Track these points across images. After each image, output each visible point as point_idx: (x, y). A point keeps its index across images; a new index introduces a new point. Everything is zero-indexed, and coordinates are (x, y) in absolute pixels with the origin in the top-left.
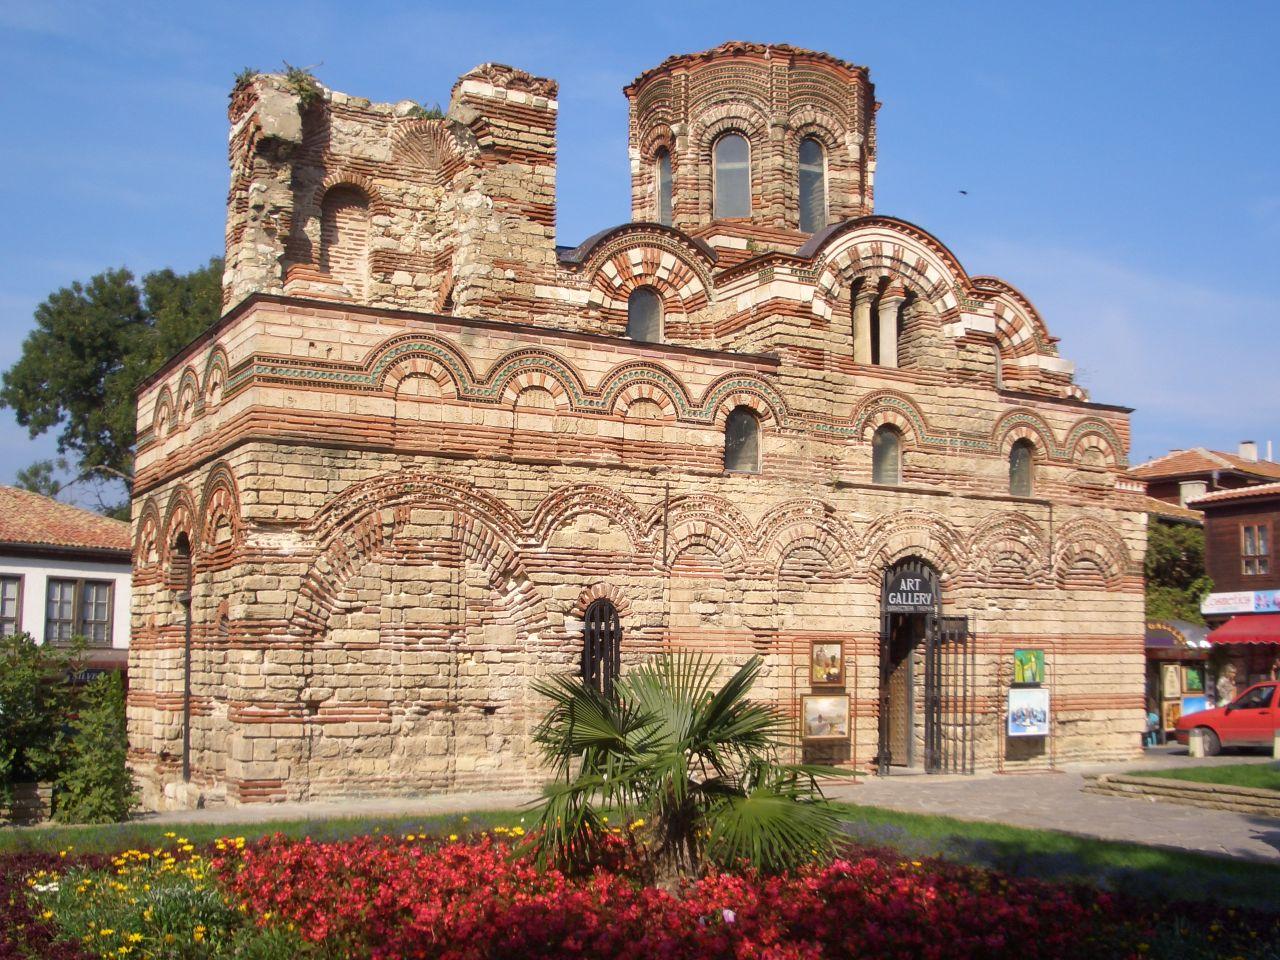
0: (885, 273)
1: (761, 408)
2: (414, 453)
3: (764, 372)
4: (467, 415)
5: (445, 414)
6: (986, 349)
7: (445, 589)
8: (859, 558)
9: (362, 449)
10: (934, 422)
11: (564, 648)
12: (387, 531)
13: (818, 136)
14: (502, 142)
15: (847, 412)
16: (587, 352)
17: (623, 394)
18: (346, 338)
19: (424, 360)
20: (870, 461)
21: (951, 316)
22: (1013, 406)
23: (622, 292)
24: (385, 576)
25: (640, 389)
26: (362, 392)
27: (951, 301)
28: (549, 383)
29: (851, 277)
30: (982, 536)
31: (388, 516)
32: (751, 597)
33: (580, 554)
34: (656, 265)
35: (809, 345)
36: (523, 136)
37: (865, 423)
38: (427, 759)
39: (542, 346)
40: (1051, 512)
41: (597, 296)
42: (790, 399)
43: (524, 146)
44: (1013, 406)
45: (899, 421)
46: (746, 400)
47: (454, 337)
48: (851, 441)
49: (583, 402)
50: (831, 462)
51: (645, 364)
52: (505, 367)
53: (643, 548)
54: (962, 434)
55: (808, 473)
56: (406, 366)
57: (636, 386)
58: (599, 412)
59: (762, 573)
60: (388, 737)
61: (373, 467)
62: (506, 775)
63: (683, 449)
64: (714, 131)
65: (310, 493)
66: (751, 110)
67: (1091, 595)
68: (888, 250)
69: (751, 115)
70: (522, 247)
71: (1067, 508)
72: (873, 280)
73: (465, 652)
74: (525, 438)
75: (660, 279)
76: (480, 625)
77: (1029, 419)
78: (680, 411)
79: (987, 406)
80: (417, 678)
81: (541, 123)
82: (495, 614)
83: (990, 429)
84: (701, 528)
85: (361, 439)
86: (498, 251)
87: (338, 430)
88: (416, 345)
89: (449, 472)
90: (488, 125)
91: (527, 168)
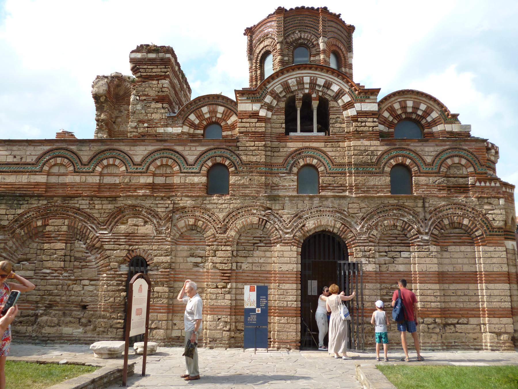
0: (307, 91)
1: (227, 163)
2: (52, 197)
3: (230, 146)
4: (77, 179)
5: (68, 179)
6: (370, 120)
7: (62, 253)
8: (287, 233)
9: (32, 196)
10: (339, 160)
11: (117, 279)
12: (41, 229)
13: (305, 44)
14: (145, 74)
15: (281, 160)
16: (135, 147)
17: (153, 164)
18: (28, 153)
19: (60, 158)
20: (296, 183)
21: (349, 105)
22: (393, 147)
23: (200, 126)
24: (39, 248)
25: (162, 161)
26: (34, 173)
27: (347, 98)
28: (117, 162)
29: (284, 96)
30: (371, 218)
31: (39, 223)
32: (219, 253)
33: (129, 236)
34: (215, 112)
35: (256, 130)
36: (153, 71)
37: (293, 164)
38: (47, 328)
39: (115, 147)
40: (424, 202)
41: (186, 129)
42: (244, 158)
43: (155, 74)
44: (393, 147)
45: (315, 162)
46: (219, 160)
47: (74, 148)
48: (284, 175)
49: (132, 169)
50: (274, 187)
51: (164, 149)
52: (97, 157)
53: (160, 233)
54: (355, 164)
55: (254, 192)
56: (52, 161)
57: (160, 160)
58: (141, 172)
59: (225, 242)
60: (34, 318)
61: (35, 203)
62: (87, 337)
63: (184, 186)
64: (260, 55)
65: (8, 215)
66: (271, 40)
67: (463, 248)
68: (307, 80)
69: (271, 43)
70: (152, 114)
71: (437, 199)
72: (301, 95)
73: (74, 280)
74: (106, 186)
75: (219, 118)
76: (81, 269)
77: (404, 152)
78: (182, 169)
79: (372, 148)
80: (46, 292)
81: (161, 64)
82: (88, 264)
83: (374, 160)
84: (192, 221)
85: (32, 192)
86: (141, 117)
87: (21, 189)
88: (57, 153)
89: (68, 203)
90: (139, 69)
91: (156, 82)
